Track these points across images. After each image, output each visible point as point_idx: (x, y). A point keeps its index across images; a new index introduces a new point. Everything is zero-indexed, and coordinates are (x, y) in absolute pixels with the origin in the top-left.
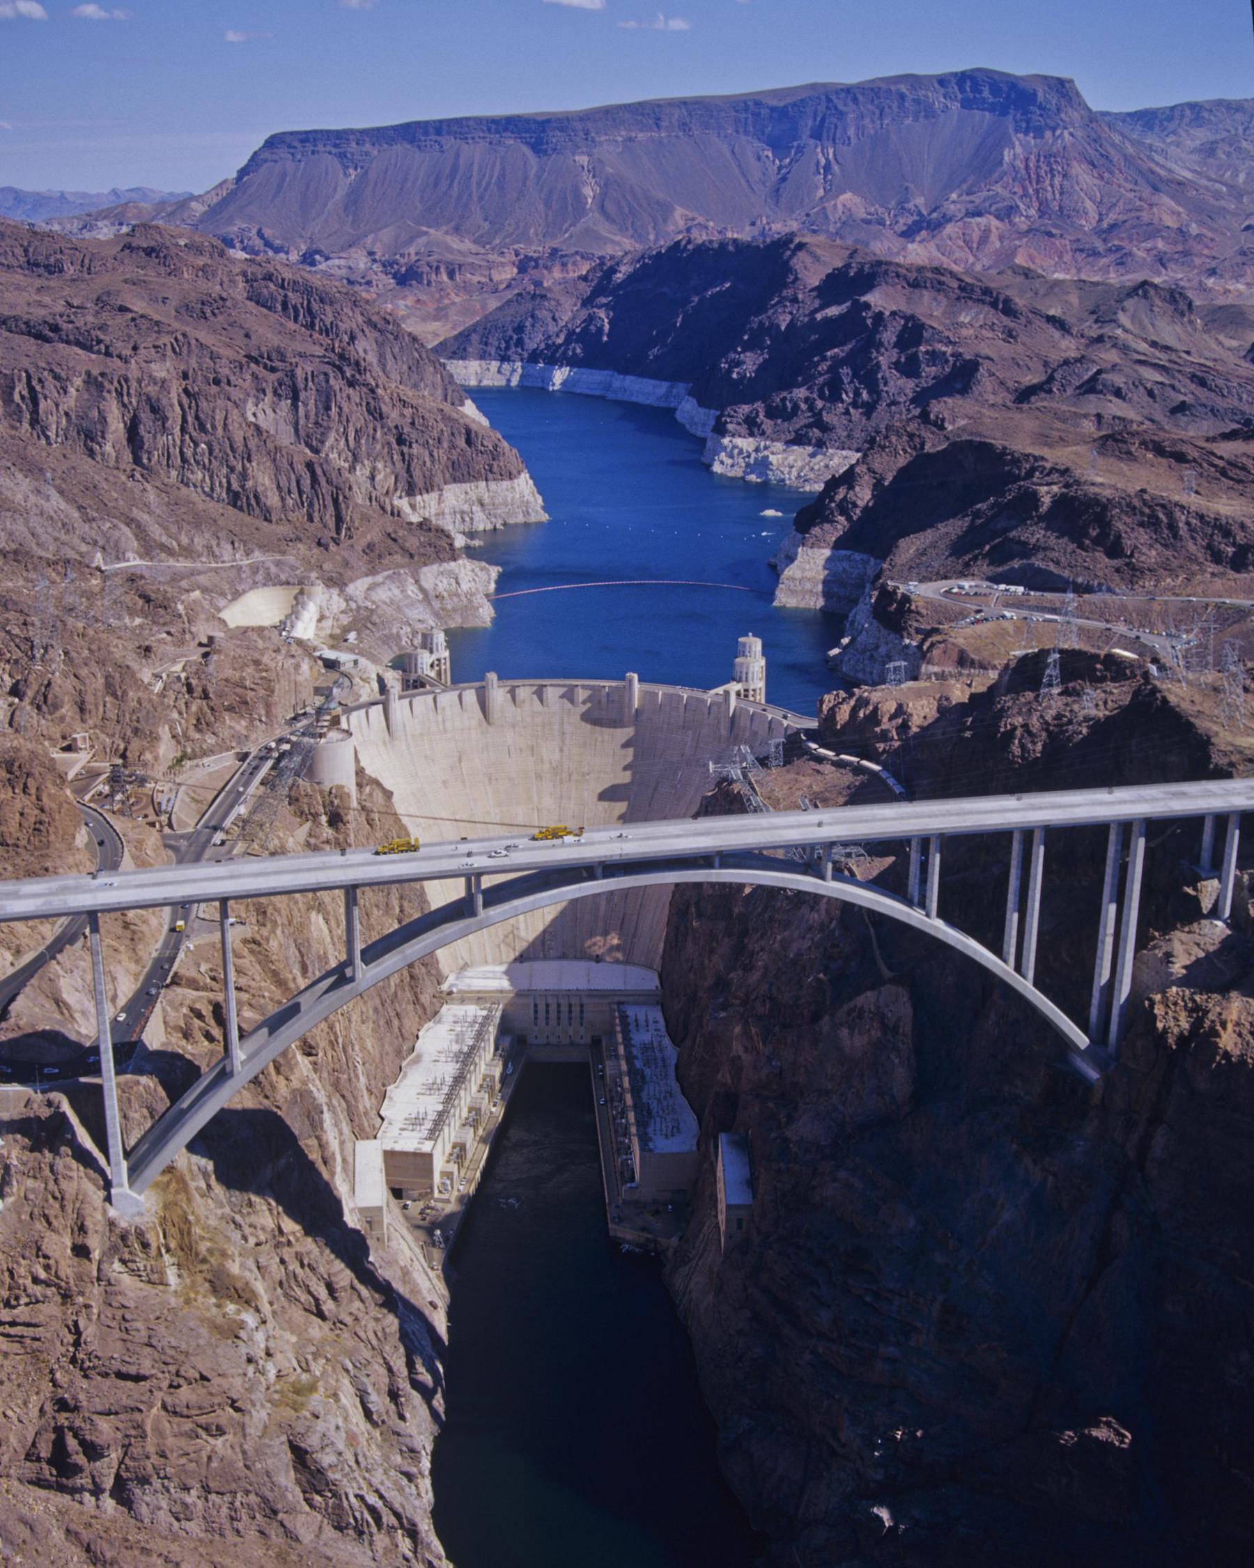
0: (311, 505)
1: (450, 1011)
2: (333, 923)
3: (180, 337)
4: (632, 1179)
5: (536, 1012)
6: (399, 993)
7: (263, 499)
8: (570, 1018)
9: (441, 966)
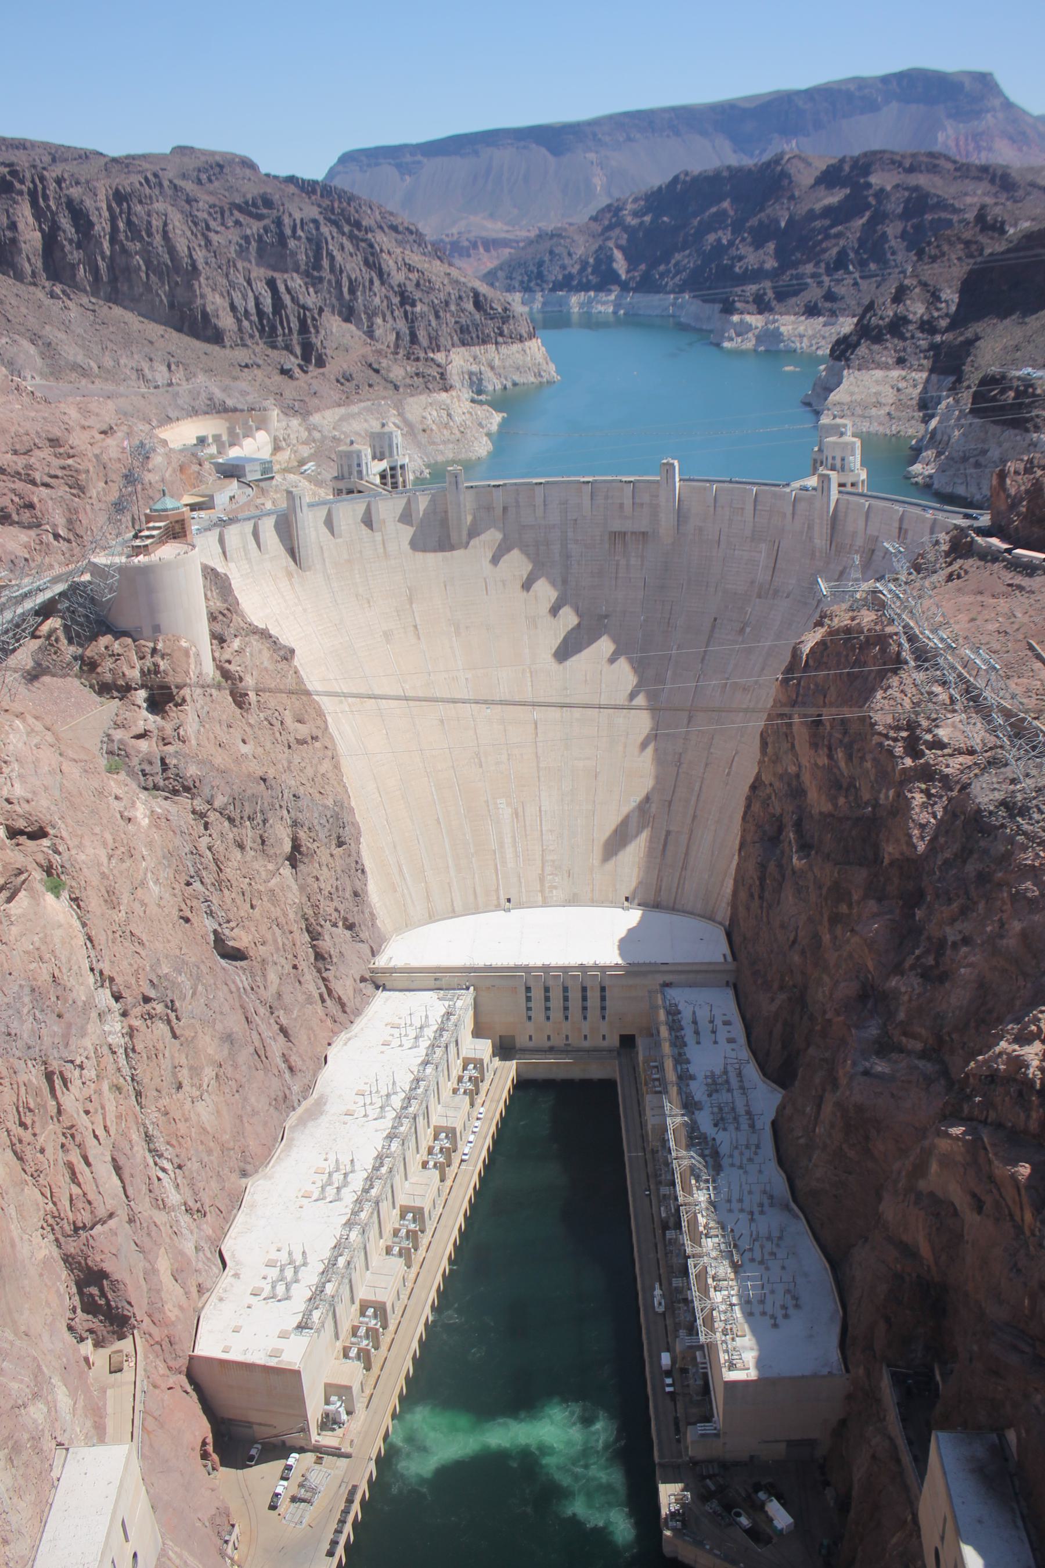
0: (273, 328)
1: (384, 1008)
2: (94, 903)
3: (150, 177)
4: (708, 1418)
5: (529, 999)
6: (286, 989)
7: (214, 320)
8: (585, 1008)
9: (378, 922)
